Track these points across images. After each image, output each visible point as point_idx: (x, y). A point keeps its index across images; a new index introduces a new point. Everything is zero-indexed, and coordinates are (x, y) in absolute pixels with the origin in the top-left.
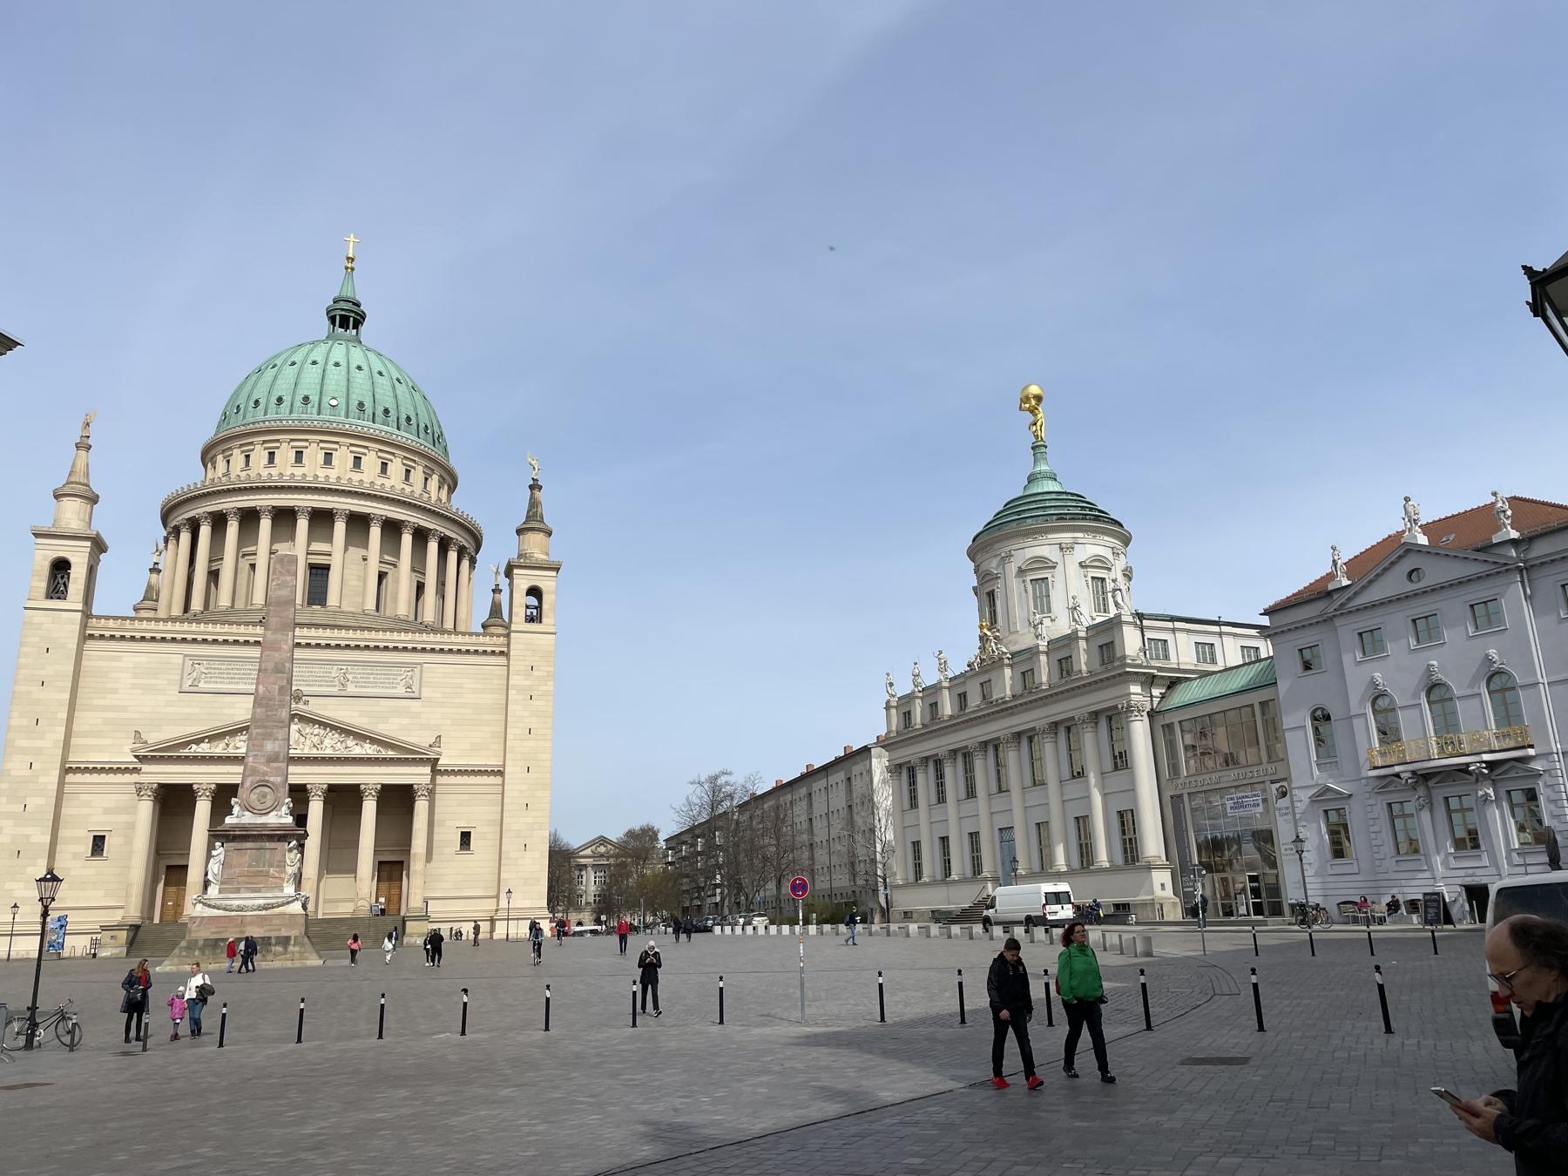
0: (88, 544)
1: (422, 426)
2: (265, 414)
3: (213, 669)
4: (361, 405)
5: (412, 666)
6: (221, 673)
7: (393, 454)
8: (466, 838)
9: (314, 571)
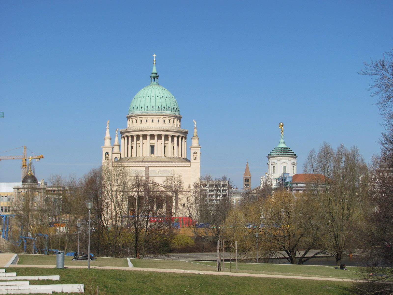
1: (172, 108)
4: (159, 107)
7: (166, 118)
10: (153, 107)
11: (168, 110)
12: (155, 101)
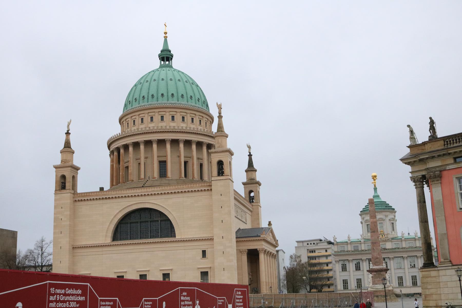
0: (70, 168)
2: (132, 106)
9: (161, 163)
10: (153, 95)
11: (179, 99)
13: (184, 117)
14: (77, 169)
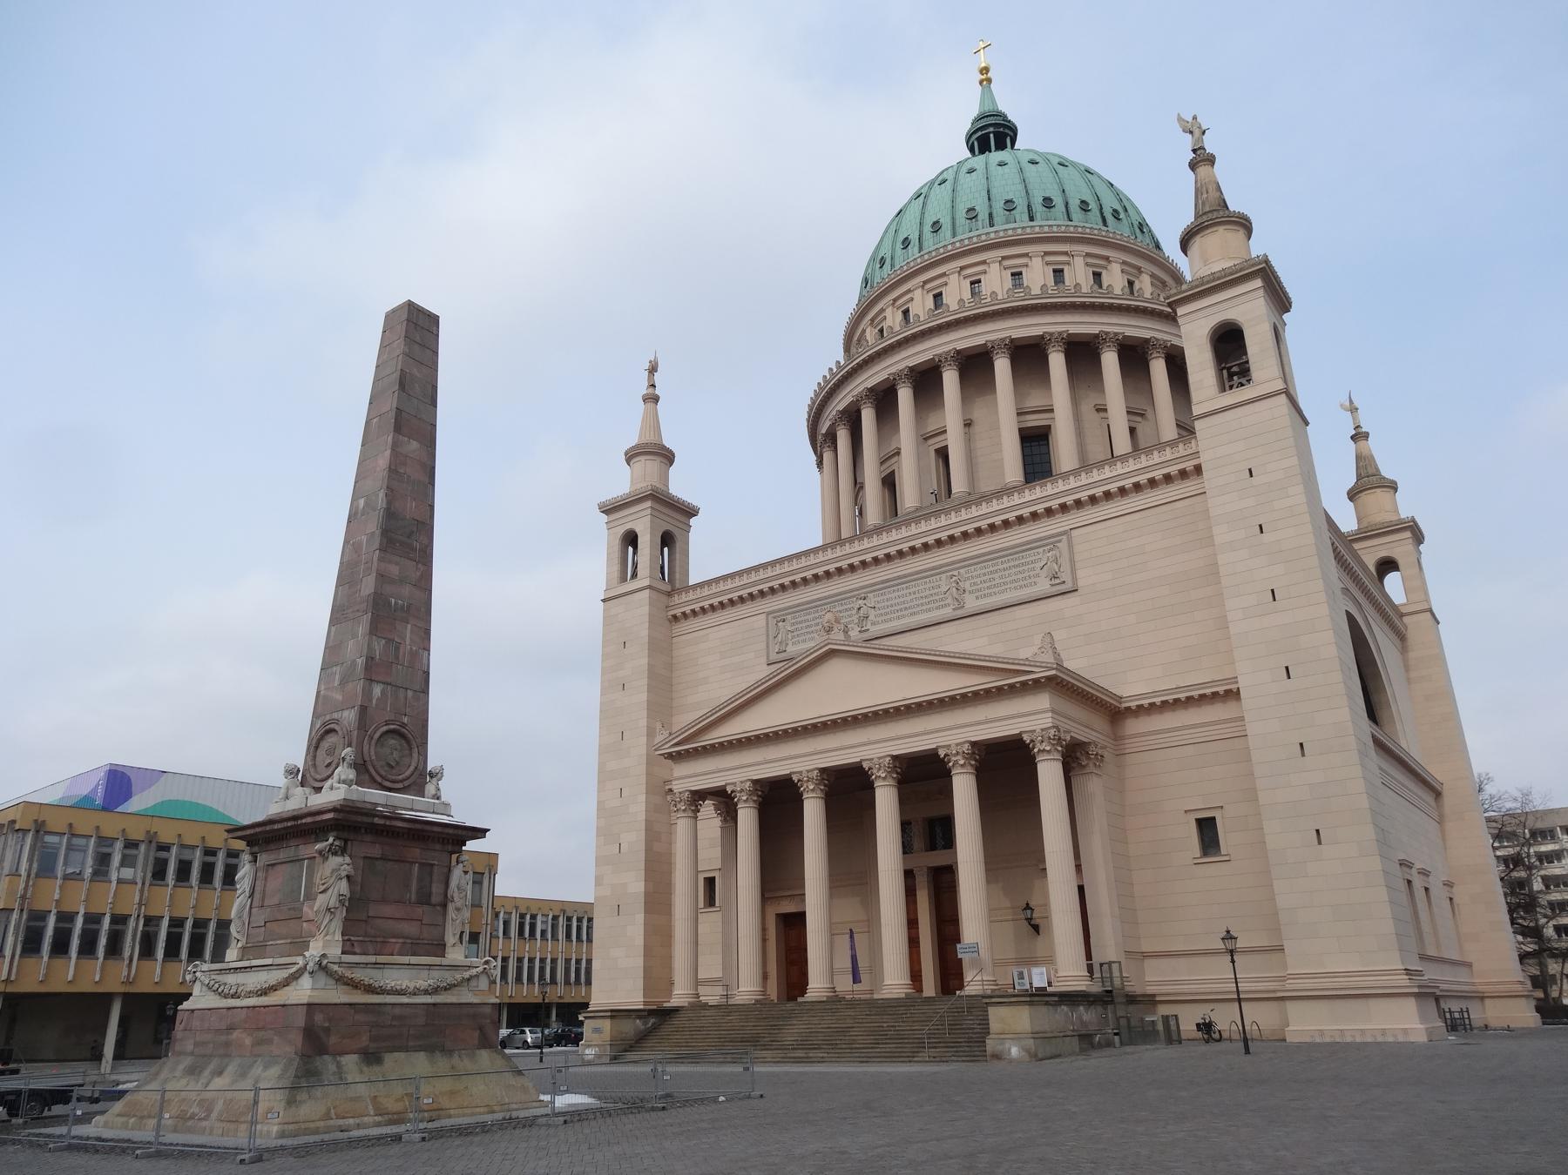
0: (648, 504)
3: (801, 622)
5: (1051, 542)
6: (807, 627)
8: (1207, 827)
12: (950, 191)
13: (1062, 271)
14: (689, 512)
